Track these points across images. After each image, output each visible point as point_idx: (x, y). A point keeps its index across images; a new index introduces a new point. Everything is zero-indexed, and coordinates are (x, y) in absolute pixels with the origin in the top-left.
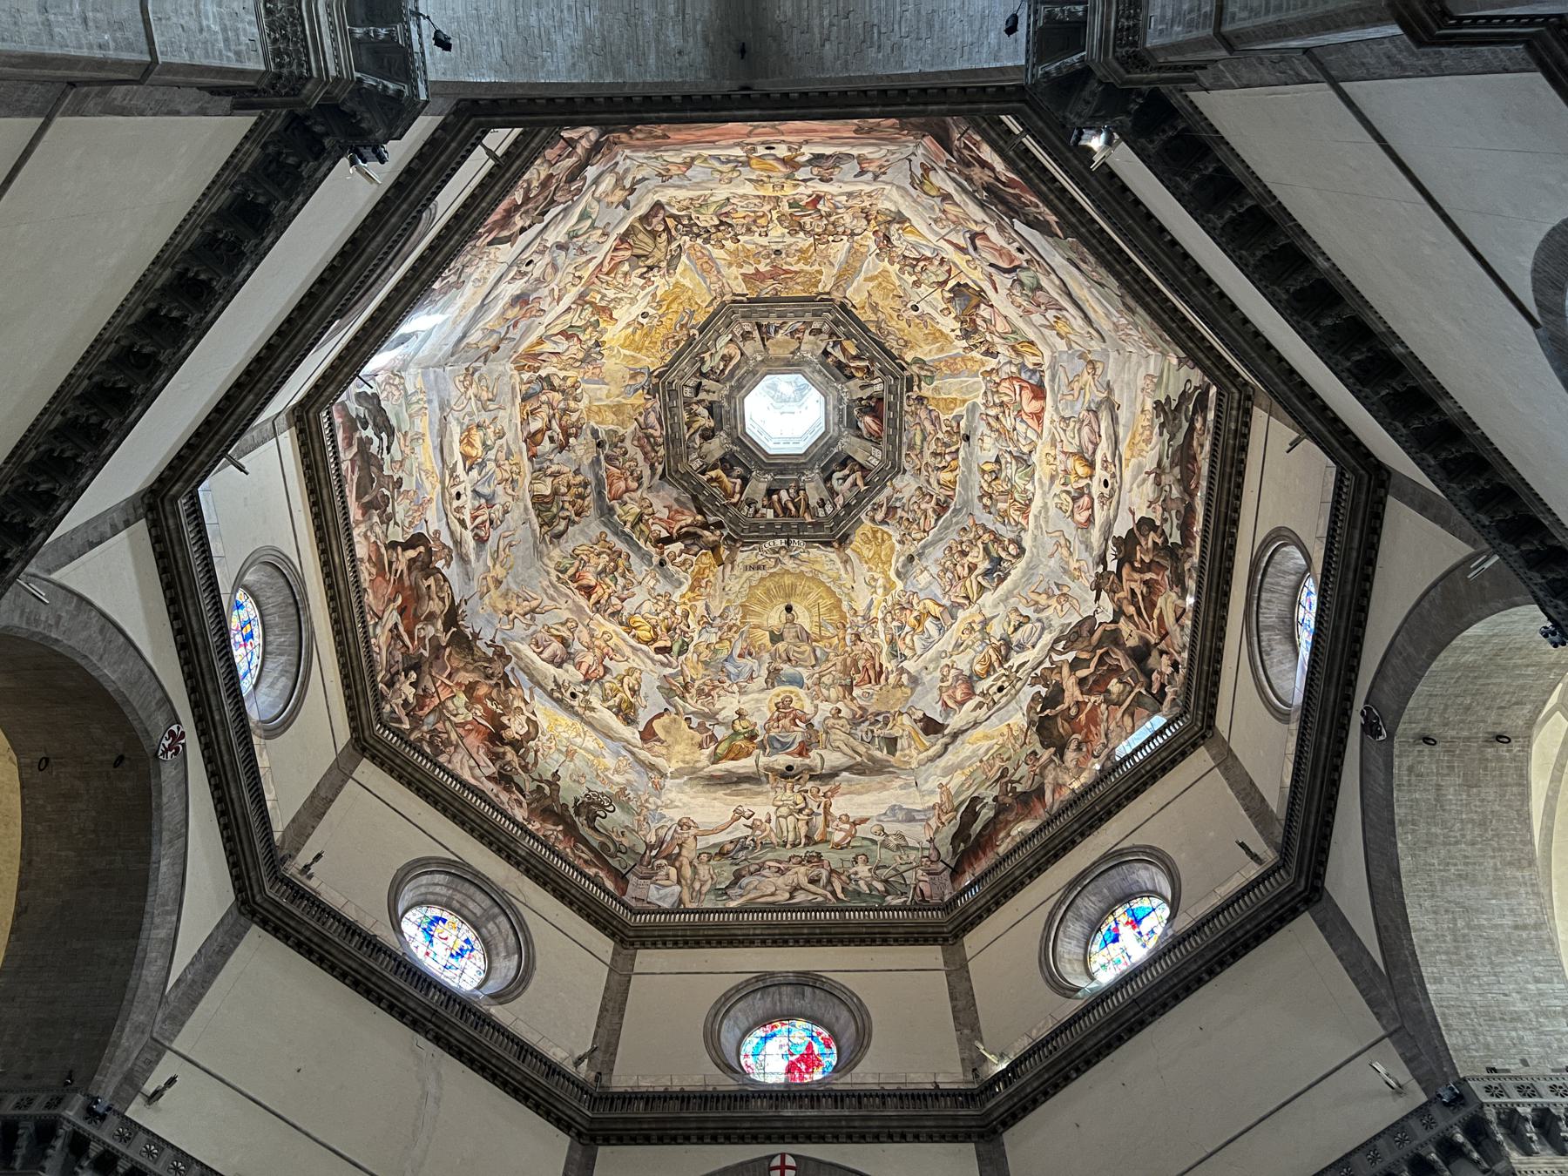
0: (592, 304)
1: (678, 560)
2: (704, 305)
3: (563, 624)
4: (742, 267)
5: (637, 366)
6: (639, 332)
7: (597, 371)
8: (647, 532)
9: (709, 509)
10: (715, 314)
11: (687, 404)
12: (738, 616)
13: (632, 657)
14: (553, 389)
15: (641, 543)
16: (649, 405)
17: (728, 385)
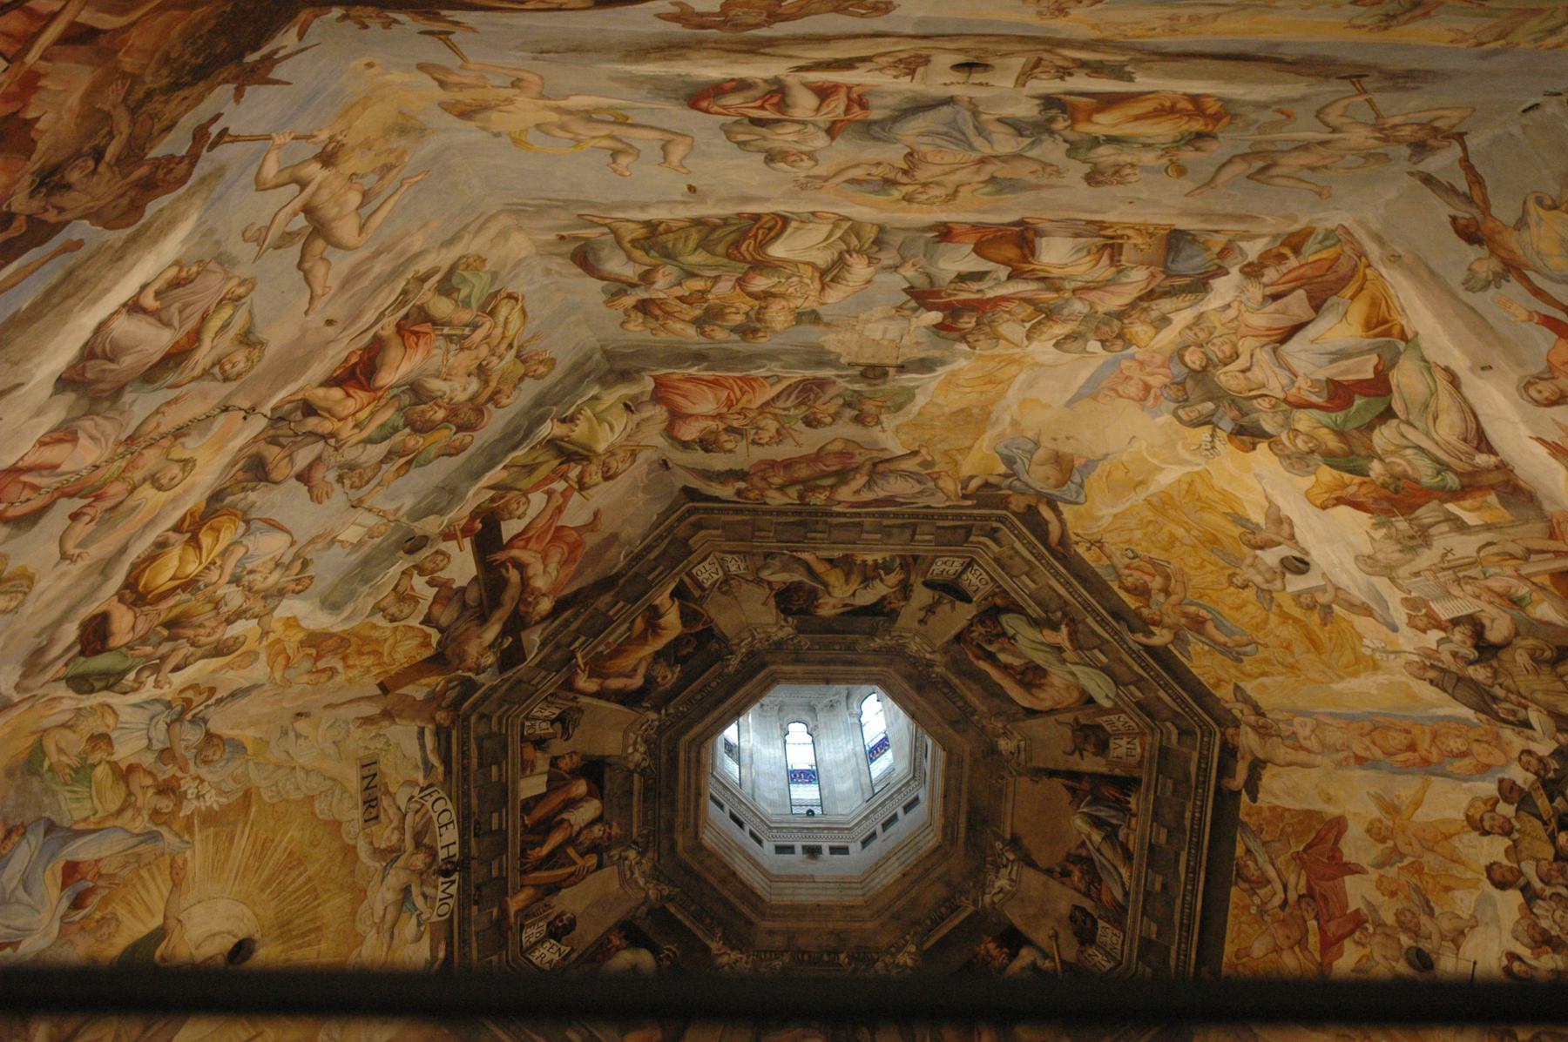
0: (1456, 495)
1: (419, 582)
2: (1249, 687)
3: (248, 339)
4: (1376, 833)
5: (1095, 482)
6: (1236, 531)
7: (1133, 389)
8: (525, 483)
9: (567, 623)
10: (1199, 693)
11: (909, 563)
12: (212, 800)
13: (75, 569)
14: (1150, 295)
15: (496, 474)
16: (949, 485)
17: (937, 657)
